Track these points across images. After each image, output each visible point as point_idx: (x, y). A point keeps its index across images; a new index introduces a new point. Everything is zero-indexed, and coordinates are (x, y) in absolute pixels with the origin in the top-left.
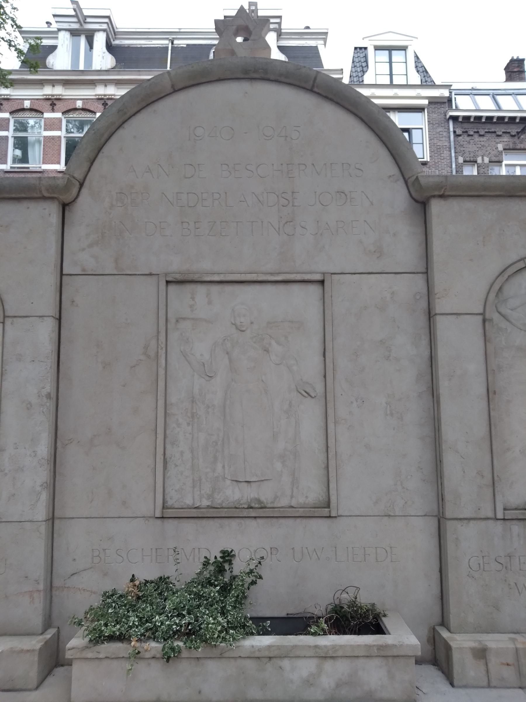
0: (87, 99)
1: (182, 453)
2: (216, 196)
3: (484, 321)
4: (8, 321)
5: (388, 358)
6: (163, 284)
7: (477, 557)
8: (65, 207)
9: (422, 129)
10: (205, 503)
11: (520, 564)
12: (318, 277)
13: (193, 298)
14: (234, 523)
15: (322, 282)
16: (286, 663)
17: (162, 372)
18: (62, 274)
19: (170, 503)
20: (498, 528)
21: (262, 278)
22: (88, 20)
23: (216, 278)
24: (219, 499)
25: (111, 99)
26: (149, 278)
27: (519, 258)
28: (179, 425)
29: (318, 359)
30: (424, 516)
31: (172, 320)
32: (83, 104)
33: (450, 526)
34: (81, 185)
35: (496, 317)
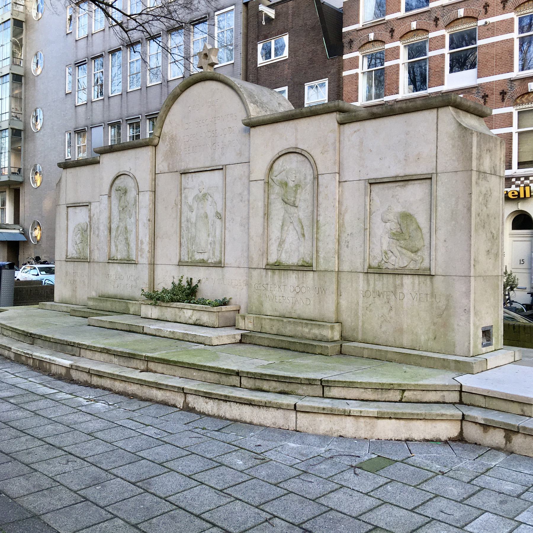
5: (241, 201)
12: (221, 167)
16: (185, 311)
19: (182, 260)
21: (205, 169)
23: (193, 171)
26: (176, 173)
31: (183, 189)
34: (159, 137)
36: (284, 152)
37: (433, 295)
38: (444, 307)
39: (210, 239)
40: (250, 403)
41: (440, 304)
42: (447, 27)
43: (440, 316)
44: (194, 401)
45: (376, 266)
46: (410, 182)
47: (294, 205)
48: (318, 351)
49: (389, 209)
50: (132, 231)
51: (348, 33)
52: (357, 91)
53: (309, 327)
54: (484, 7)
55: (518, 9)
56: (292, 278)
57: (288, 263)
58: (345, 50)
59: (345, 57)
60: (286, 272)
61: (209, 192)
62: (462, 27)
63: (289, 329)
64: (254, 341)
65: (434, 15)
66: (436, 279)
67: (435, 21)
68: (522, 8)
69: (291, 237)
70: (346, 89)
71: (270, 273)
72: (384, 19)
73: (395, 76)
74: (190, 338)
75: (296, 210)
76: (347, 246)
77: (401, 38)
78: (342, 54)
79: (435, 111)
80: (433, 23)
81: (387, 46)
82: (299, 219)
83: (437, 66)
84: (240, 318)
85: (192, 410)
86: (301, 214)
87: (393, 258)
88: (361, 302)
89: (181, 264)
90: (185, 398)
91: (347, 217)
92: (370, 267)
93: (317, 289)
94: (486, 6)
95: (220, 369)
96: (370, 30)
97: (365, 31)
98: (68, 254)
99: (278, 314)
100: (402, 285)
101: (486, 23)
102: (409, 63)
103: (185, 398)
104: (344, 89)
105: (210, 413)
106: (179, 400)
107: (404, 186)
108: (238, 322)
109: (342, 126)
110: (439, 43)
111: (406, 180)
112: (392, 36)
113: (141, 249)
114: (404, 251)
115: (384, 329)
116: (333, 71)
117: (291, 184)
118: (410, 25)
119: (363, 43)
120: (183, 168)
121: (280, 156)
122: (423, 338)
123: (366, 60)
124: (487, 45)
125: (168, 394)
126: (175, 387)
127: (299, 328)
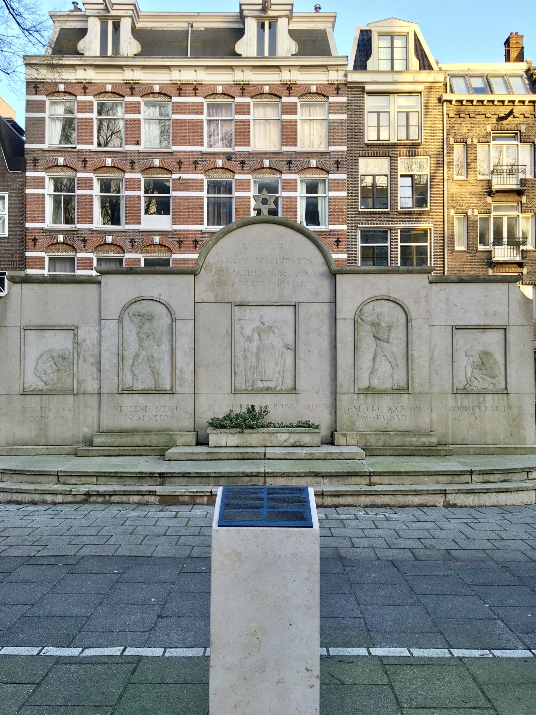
0: (115, 83)
1: (241, 371)
2: (254, 271)
4: (177, 321)
5: (319, 335)
6: (233, 306)
8: (195, 275)
9: (418, 112)
10: (250, 388)
12: (293, 304)
13: (245, 312)
14: (261, 395)
15: (295, 306)
16: (278, 435)
17: (233, 340)
18: (195, 303)
20: (356, 396)
22: (115, 7)
23: (254, 304)
24: (255, 387)
25: (138, 83)
28: (240, 360)
29: (292, 335)
31: (237, 320)
32: (113, 88)
33: (338, 395)
34: (201, 267)
35: (359, 320)
37: (509, 406)
38: (517, 414)
39: (278, 368)
40: (507, 491)
41: (514, 413)
42: (143, 171)
43: (514, 420)
44: (451, 498)
45: (462, 388)
46: (488, 330)
47: (388, 342)
48: (443, 453)
49: (471, 347)
50: (163, 359)
51: (32, 150)
52: (44, 212)
53: (417, 437)
54: (178, 163)
55: (207, 173)
56: (387, 400)
57: (381, 388)
58: (28, 167)
59: (28, 174)
60: (380, 395)
61: (274, 324)
62: (157, 176)
63: (407, 440)
64: (375, 453)
65: (130, 158)
66: (510, 395)
67: (130, 163)
68: (210, 172)
69: (384, 367)
70: (30, 208)
71: (362, 396)
72: (75, 148)
73: (89, 206)
74: (334, 457)
75: (389, 345)
76: (437, 374)
77: (95, 170)
78: (25, 171)
79: (507, 284)
80: (129, 166)
81: (79, 175)
82: (393, 353)
83: (134, 206)
84: (340, 436)
85: (454, 506)
86: (394, 349)
87: (477, 382)
88: (450, 416)
89: (236, 392)
90: (446, 498)
91: (436, 353)
92: (457, 390)
93: (413, 407)
94: (180, 163)
95: (455, 471)
96: (59, 154)
97: (54, 153)
98: (26, 386)
99: (372, 430)
100: (485, 401)
101: (180, 178)
102: (101, 196)
103: (446, 498)
104: (28, 207)
105: (472, 505)
106: (440, 500)
107: (484, 332)
108: (338, 440)
109: (430, 284)
110: (134, 185)
111: (485, 328)
112: (85, 166)
113: (182, 378)
114: (486, 377)
115: (471, 432)
116: (16, 185)
117: (383, 324)
118: (105, 161)
119: (50, 165)
120: (238, 300)
122: (502, 436)
123: (52, 183)
124: (181, 198)
125: (426, 497)
126: (436, 490)
127: (407, 439)
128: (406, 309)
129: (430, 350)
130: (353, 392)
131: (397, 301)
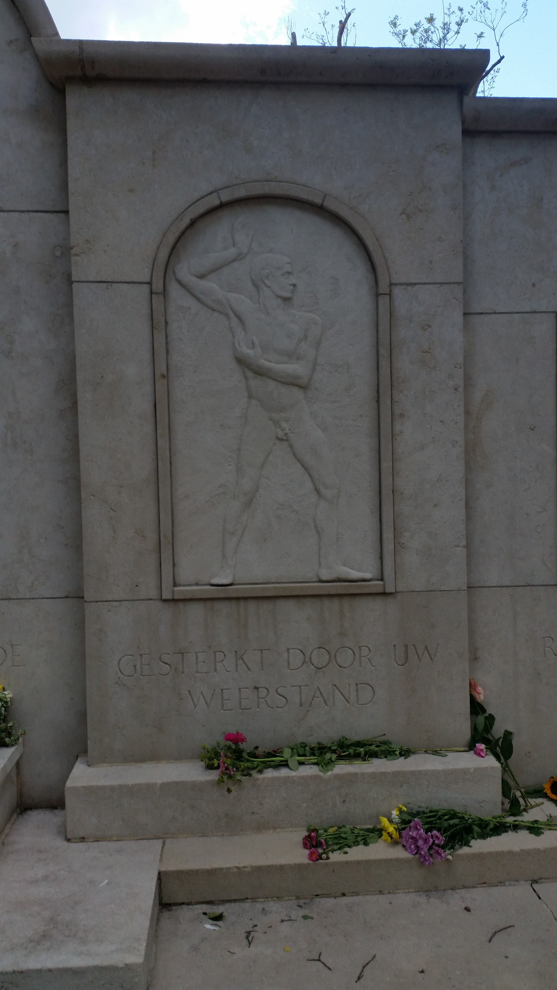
3: (151, 293)
7: (132, 657)
11: (197, 664)
27: (211, 189)
30: (67, 597)
36: (241, 193)
121: (222, 206)
128: (369, 243)
129: (467, 413)
130: (153, 593)
131: (330, 204)
